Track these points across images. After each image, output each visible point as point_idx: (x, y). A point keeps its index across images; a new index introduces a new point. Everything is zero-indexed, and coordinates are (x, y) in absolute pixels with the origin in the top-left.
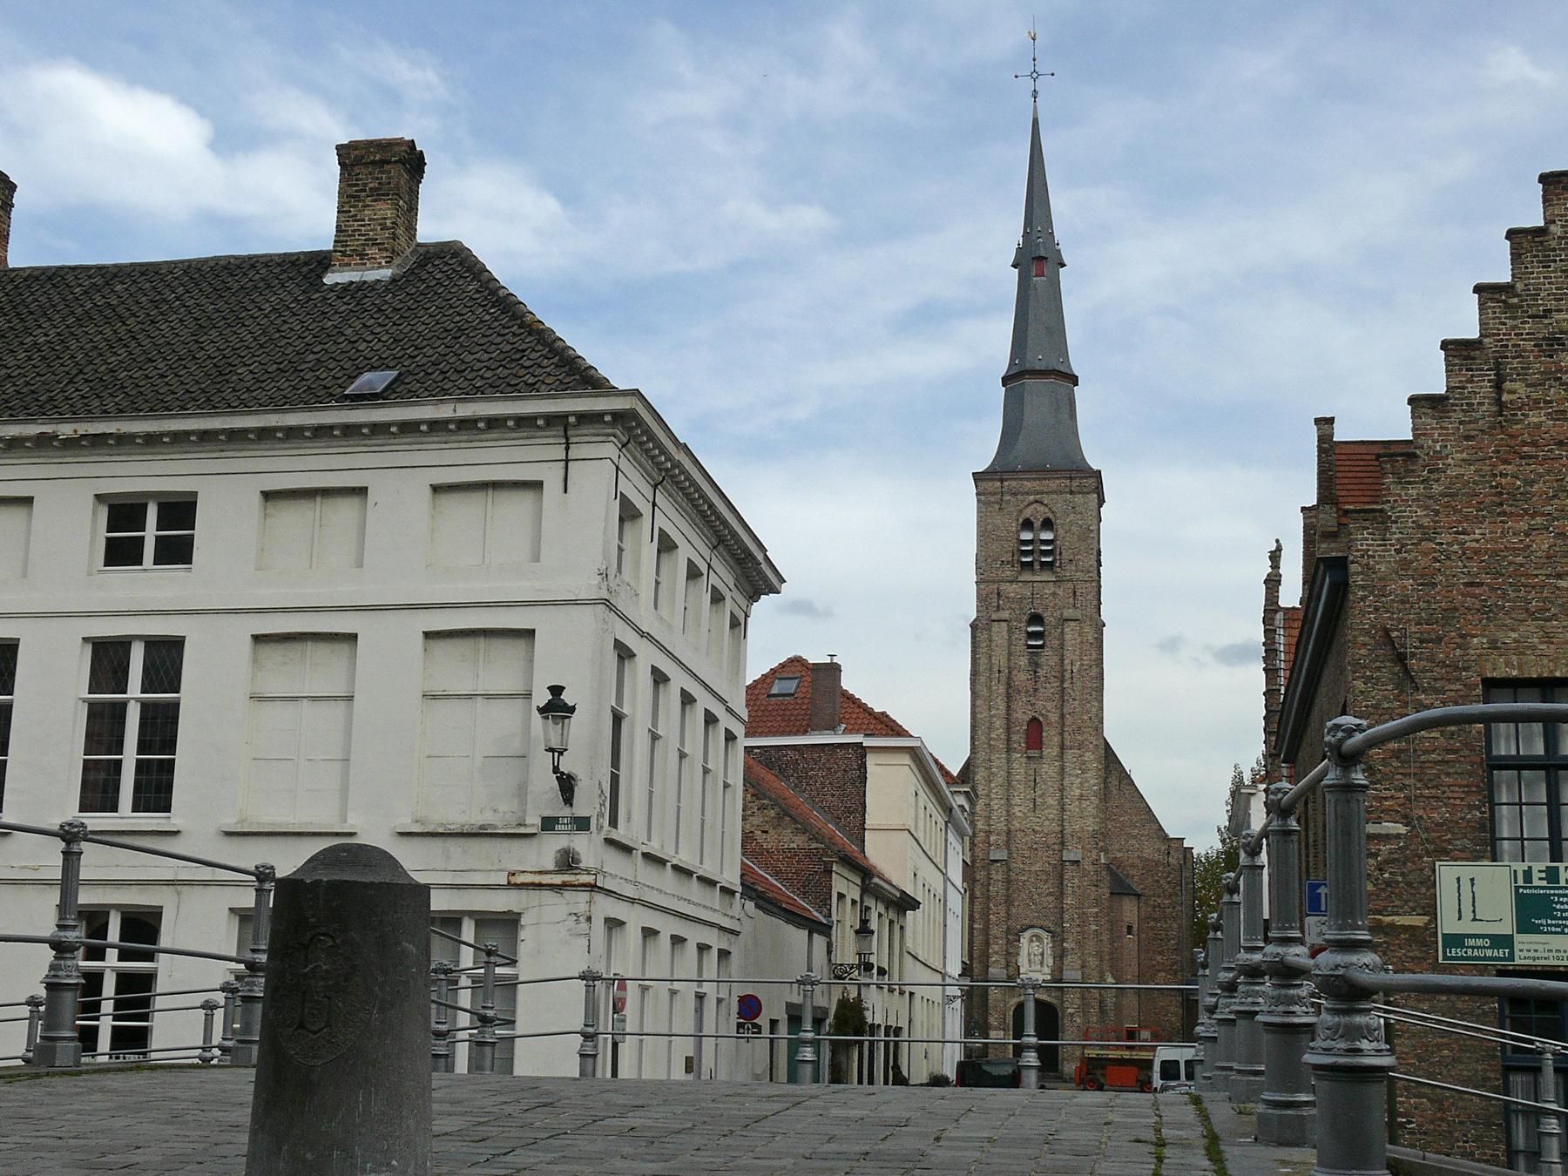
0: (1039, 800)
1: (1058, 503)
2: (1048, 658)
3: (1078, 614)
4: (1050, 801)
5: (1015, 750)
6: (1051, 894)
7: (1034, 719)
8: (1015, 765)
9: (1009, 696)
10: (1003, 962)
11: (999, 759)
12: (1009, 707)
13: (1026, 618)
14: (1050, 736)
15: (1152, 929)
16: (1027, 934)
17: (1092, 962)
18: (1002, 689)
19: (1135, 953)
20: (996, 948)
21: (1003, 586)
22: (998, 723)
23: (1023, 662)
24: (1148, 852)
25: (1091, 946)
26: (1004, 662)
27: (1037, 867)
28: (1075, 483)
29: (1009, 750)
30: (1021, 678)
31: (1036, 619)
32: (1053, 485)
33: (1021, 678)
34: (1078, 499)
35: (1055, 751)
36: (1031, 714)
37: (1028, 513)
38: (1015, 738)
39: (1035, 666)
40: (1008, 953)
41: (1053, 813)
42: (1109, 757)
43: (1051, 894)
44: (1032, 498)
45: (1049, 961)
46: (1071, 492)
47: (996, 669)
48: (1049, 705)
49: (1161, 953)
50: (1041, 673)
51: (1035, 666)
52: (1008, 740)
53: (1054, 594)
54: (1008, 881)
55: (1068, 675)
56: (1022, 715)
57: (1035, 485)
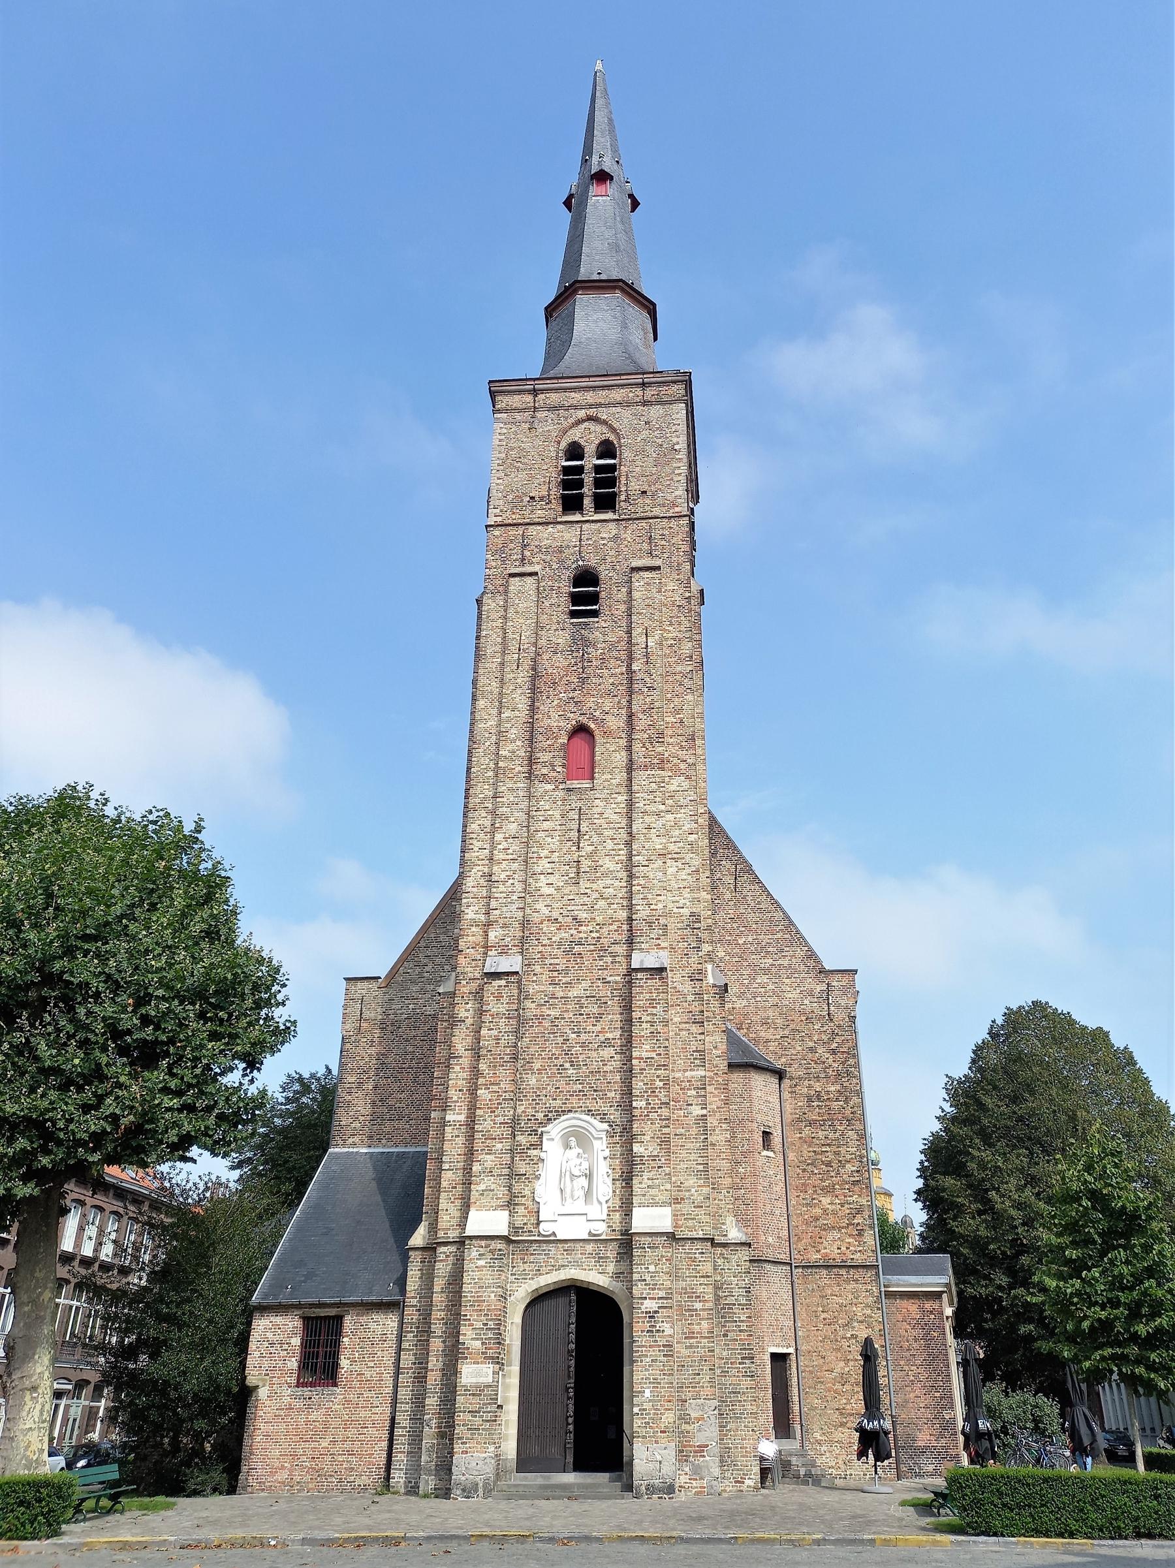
0: (585, 864)
1: (623, 419)
3: (658, 562)
4: (609, 864)
6: (607, 1043)
7: (581, 730)
9: (534, 689)
10: (502, 1192)
11: (513, 789)
13: (568, 574)
14: (610, 754)
15: (809, 1142)
16: (555, 1131)
17: (694, 1187)
18: (523, 677)
19: (779, 1188)
20: (489, 1160)
21: (532, 530)
22: (513, 733)
23: (562, 639)
26: (527, 636)
28: (650, 392)
29: (530, 776)
30: (556, 664)
31: (586, 578)
32: (617, 395)
33: (556, 664)
34: (655, 412)
36: (574, 719)
37: (576, 435)
39: (581, 644)
40: (513, 1175)
41: (615, 887)
42: (713, 822)
43: (607, 1043)
45: (605, 1188)
46: (645, 403)
47: (513, 647)
49: (829, 1190)
51: (581, 644)
52: (531, 761)
54: (520, 1021)
55: (638, 653)
56: (556, 719)
57: (590, 397)
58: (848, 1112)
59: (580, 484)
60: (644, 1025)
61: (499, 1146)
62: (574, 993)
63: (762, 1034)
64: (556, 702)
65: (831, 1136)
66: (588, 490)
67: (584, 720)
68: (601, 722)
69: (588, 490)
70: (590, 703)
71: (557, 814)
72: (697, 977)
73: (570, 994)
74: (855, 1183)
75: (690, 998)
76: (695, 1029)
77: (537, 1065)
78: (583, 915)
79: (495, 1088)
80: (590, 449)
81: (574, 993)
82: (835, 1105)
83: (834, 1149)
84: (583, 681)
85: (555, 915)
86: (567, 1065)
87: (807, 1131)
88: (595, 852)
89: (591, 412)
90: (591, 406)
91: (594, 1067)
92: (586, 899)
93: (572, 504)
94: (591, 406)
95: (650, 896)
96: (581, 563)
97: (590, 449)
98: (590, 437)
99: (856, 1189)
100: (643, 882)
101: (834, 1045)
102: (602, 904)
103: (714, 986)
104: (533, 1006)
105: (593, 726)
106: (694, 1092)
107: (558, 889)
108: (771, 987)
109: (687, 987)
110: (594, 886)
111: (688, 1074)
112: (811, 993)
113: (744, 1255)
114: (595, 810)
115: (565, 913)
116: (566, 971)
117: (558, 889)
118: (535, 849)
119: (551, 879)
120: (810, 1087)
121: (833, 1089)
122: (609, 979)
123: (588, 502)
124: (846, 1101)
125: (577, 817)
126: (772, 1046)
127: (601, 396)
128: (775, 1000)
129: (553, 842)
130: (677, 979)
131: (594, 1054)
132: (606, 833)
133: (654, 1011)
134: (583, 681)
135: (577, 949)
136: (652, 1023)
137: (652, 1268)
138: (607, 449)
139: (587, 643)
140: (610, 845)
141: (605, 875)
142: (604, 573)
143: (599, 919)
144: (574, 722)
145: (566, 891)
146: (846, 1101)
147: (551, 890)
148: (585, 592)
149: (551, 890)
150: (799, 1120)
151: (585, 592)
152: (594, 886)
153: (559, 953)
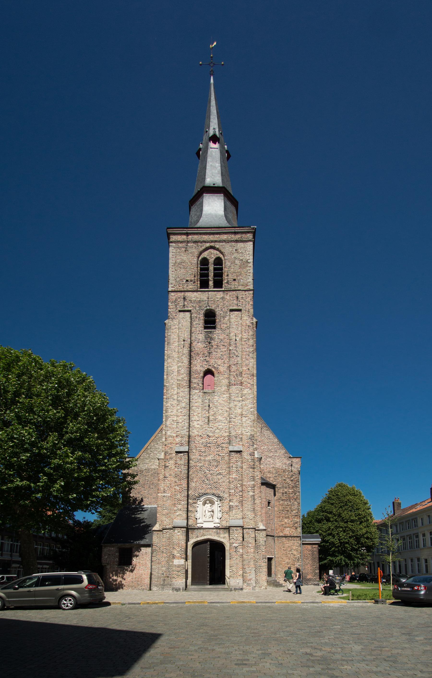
0: (211, 418)
2: (218, 334)
4: (220, 418)
5: (195, 388)
8: (195, 397)
12: (190, 363)
15: (282, 505)
23: (201, 337)
24: (279, 464)
25: (248, 505)
27: (209, 458)
33: (199, 346)
35: (224, 388)
36: (206, 367)
38: (194, 381)
44: (208, 245)
48: (220, 362)
49: (288, 518)
50: (213, 343)
53: (223, 298)
57: (211, 237)
58: (295, 497)
59: (207, 275)
60: (234, 468)
61: (183, 503)
62: (207, 459)
63: (268, 475)
64: (199, 361)
65: (289, 503)
66: (211, 277)
67: (210, 368)
68: (216, 369)
69: (211, 277)
70: (212, 361)
71: (200, 400)
72: (252, 454)
73: (206, 459)
74: (295, 516)
75: (250, 461)
76: (251, 470)
77: (195, 480)
78: (211, 434)
79: (181, 486)
80: (211, 261)
81: (207, 459)
82: (291, 495)
83: (290, 507)
84: (210, 353)
85: (200, 434)
86: (206, 480)
87: (281, 502)
88: (215, 413)
89: (212, 244)
90: (212, 242)
91: (216, 481)
92: (211, 429)
93: (204, 284)
94: (212, 242)
95: (236, 428)
96: (208, 308)
97: (211, 261)
98: (211, 255)
99: (296, 517)
100: (233, 424)
101: (292, 479)
102: (217, 431)
103: (257, 458)
104: (193, 462)
105: (213, 370)
106: (250, 488)
107: (201, 426)
108: (272, 462)
109: (249, 457)
110: (215, 425)
111: (249, 483)
112: (285, 464)
113: (264, 533)
114: (215, 400)
115: (204, 433)
116: (205, 452)
117: (201, 426)
118: (192, 412)
119: (198, 422)
120: (283, 490)
121: (290, 491)
122: (220, 454)
123: (211, 283)
124: (295, 494)
125: (208, 402)
126: (271, 479)
127: (216, 237)
128: (273, 466)
129: (200, 410)
130: (245, 455)
131: (216, 477)
132: (219, 408)
133: (238, 464)
134: (210, 353)
135: (208, 445)
136: (237, 468)
137: (236, 535)
138: (218, 262)
139: (211, 339)
140: (221, 411)
141: (219, 421)
142: (218, 312)
143: (217, 436)
144: (206, 369)
145: (205, 426)
146: (295, 494)
147: (198, 426)
148: (210, 320)
149: (198, 426)
150: (279, 499)
151: (210, 320)
152: (215, 425)
153: (202, 446)
